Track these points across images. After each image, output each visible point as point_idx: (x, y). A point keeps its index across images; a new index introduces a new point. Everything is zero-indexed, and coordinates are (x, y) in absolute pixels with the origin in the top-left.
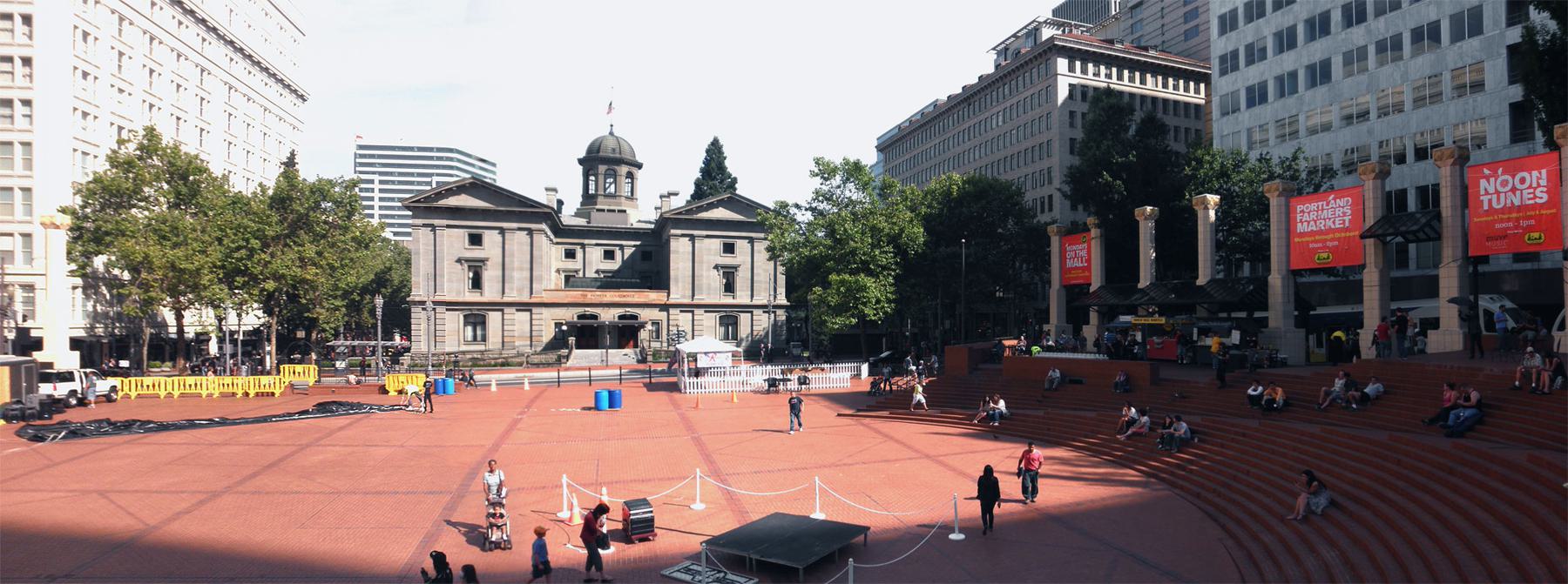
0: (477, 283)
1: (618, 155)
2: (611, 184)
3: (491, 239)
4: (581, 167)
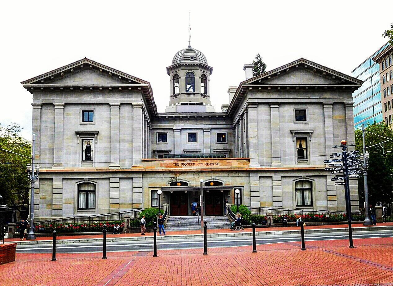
1: (195, 61)
3: (100, 114)
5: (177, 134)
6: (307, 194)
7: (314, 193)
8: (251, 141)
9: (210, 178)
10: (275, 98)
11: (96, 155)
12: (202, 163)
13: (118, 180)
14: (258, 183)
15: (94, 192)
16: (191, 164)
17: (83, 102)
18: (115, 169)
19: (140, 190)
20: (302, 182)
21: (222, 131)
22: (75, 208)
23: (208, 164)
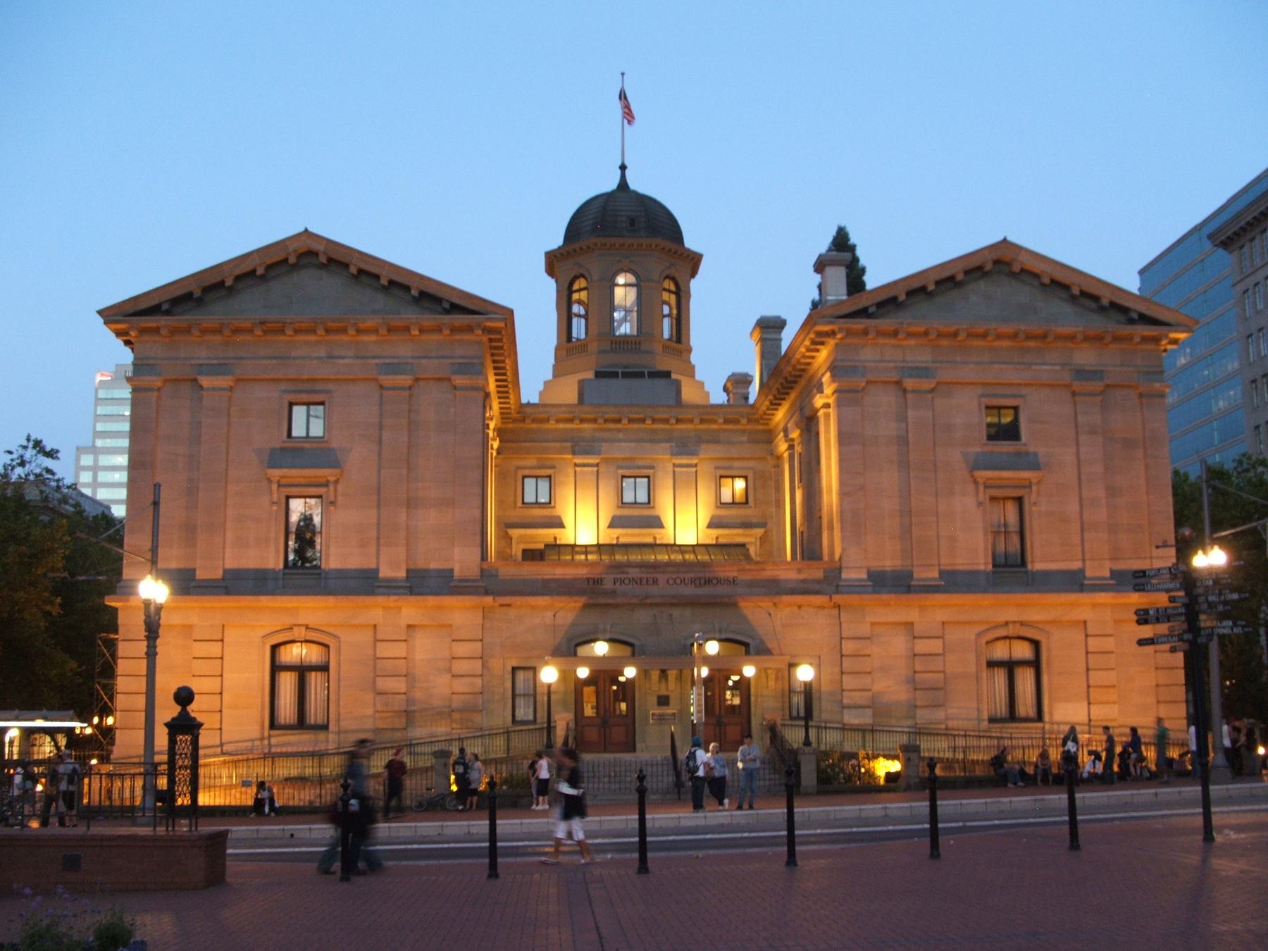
6: (1025, 680)
12: (682, 576)
16: (645, 581)
23: (703, 581)
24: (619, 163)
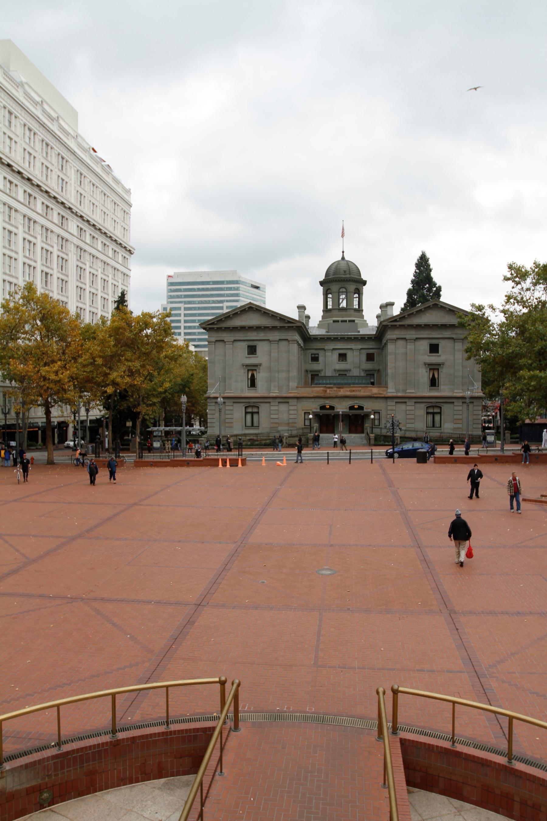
0: (253, 383)
1: (348, 276)
2: (343, 299)
3: (262, 348)
4: (322, 288)
5: (329, 354)
6: (437, 418)
7: (442, 417)
8: (390, 371)
9: (354, 403)
10: (411, 334)
11: (259, 383)
13: (277, 404)
14: (394, 408)
15: (258, 413)
17: (248, 338)
18: (275, 395)
19: (295, 412)
20: (433, 407)
21: (371, 351)
22: (243, 426)
24: (342, 251)
